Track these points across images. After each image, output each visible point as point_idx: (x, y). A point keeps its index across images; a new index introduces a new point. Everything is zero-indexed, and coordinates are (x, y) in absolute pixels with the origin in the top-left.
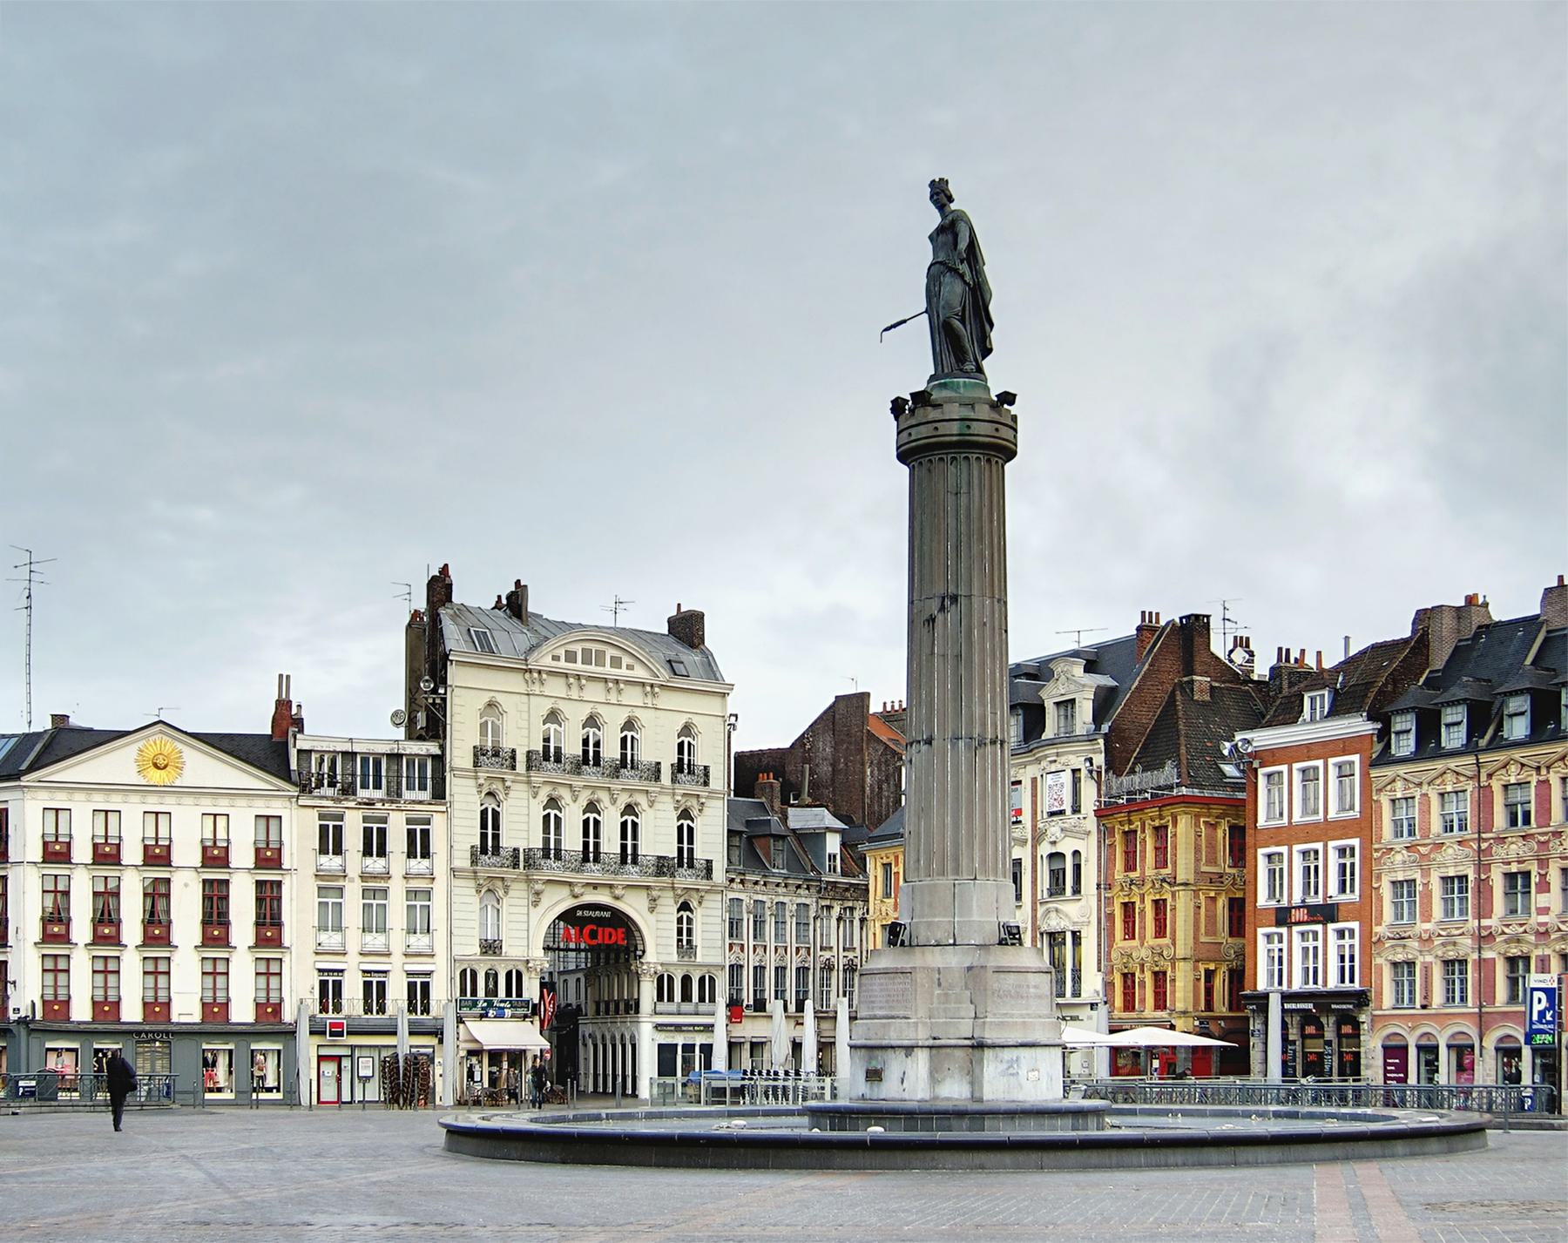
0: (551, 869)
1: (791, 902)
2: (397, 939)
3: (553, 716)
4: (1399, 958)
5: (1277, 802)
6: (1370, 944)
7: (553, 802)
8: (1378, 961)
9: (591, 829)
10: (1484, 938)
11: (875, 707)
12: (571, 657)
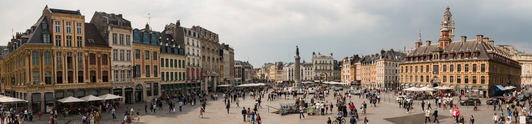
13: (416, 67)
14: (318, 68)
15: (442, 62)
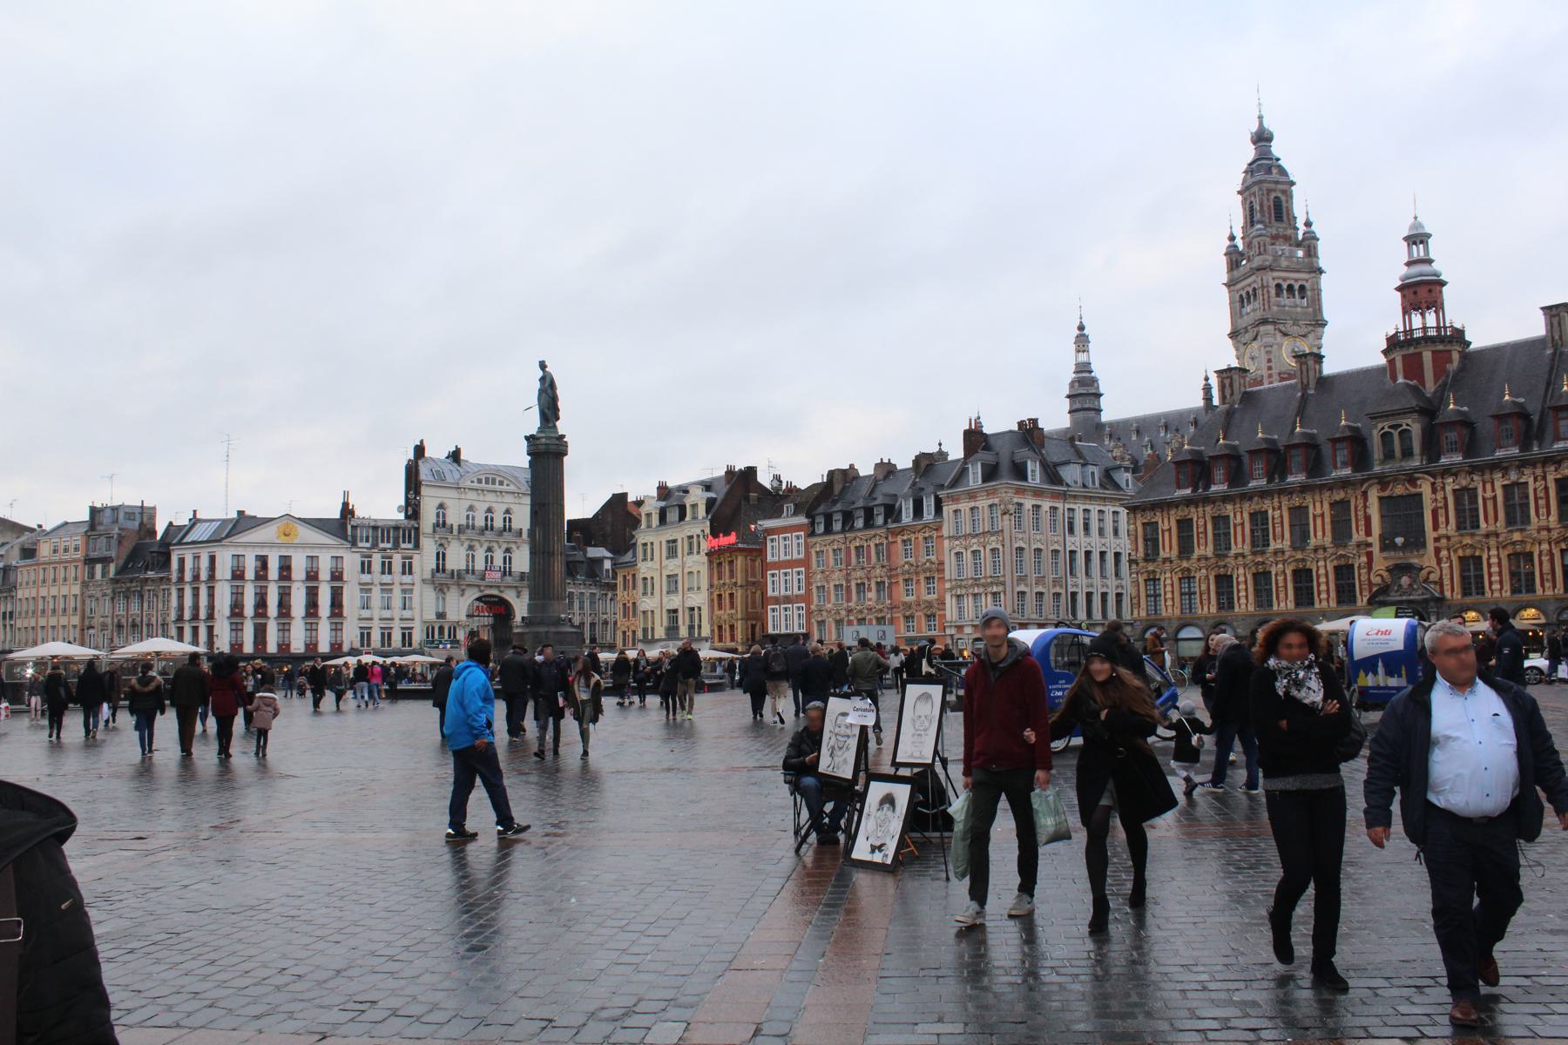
0: (470, 578)
1: (587, 592)
2: (397, 611)
3: (471, 508)
5: (776, 550)
6: (809, 613)
7: (471, 548)
9: (489, 560)
10: (849, 611)
11: (631, 499)
12: (480, 481)
13: (1259, 519)
14: (456, 558)
15: (1447, 471)
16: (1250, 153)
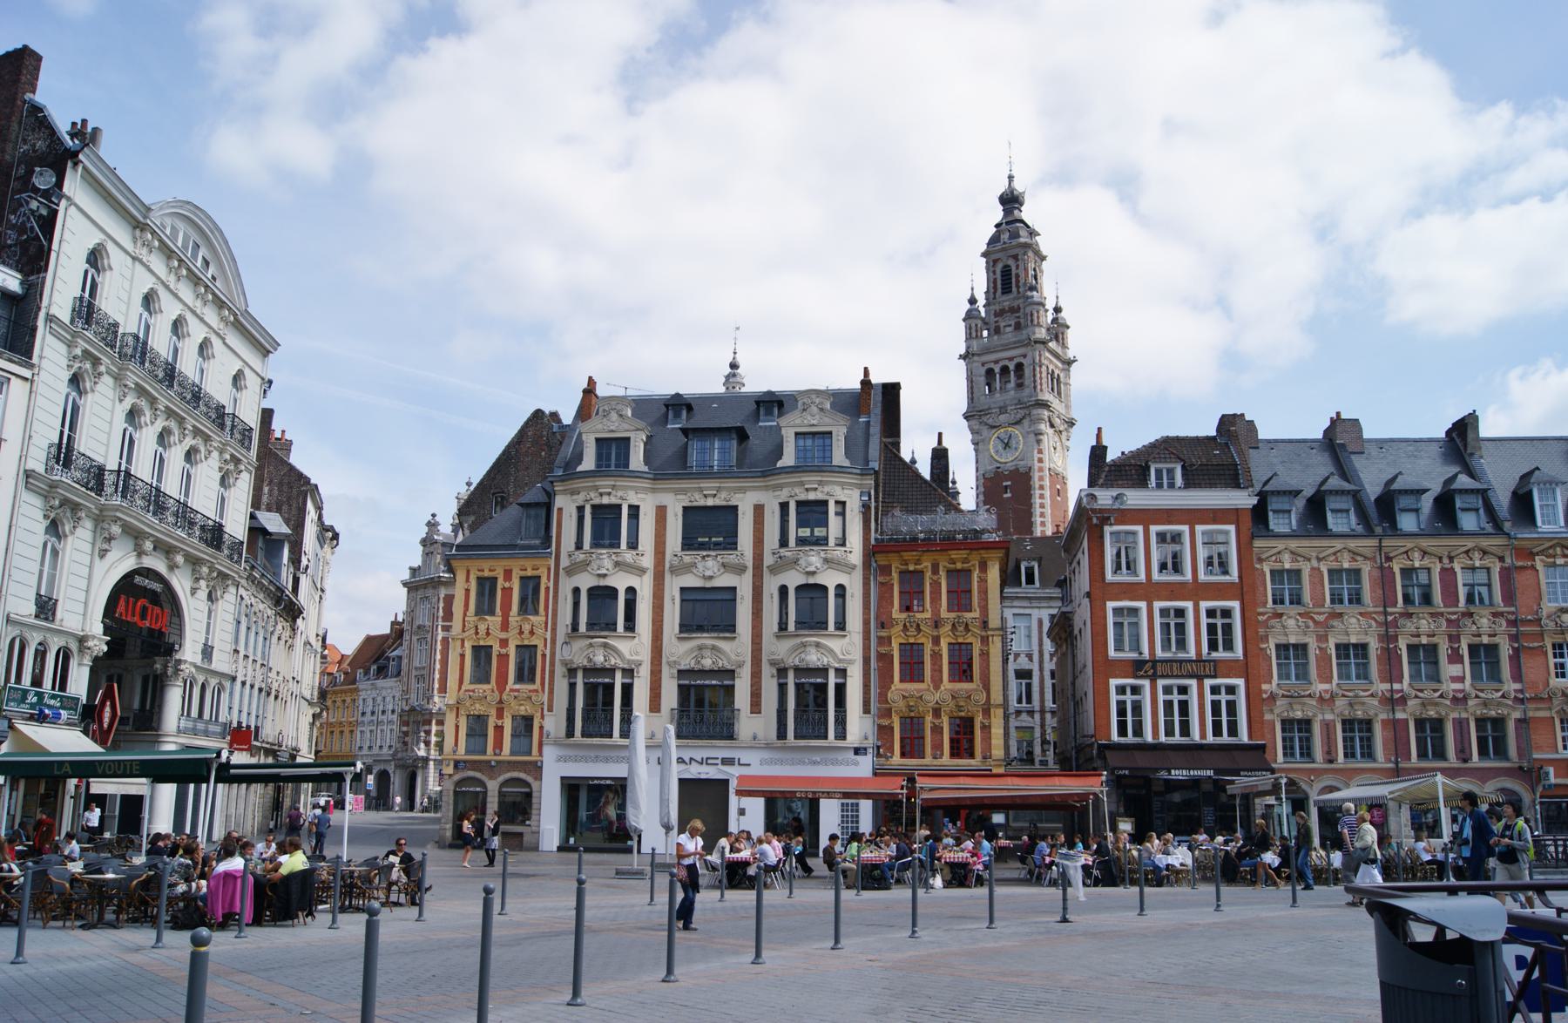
4: (1299, 715)
7: (133, 415)
8: (1268, 717)
16: (998, 214)
